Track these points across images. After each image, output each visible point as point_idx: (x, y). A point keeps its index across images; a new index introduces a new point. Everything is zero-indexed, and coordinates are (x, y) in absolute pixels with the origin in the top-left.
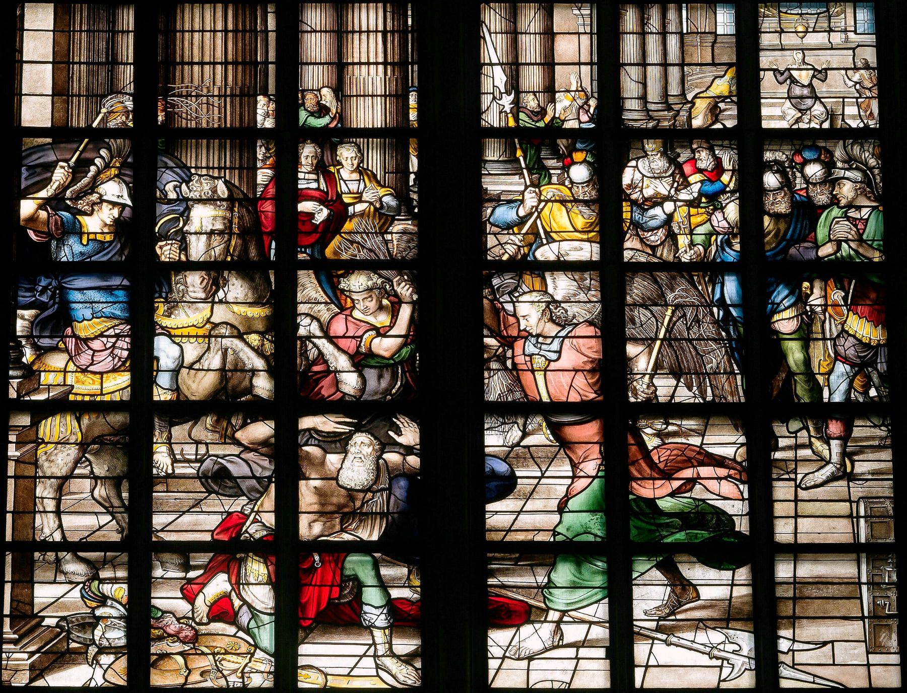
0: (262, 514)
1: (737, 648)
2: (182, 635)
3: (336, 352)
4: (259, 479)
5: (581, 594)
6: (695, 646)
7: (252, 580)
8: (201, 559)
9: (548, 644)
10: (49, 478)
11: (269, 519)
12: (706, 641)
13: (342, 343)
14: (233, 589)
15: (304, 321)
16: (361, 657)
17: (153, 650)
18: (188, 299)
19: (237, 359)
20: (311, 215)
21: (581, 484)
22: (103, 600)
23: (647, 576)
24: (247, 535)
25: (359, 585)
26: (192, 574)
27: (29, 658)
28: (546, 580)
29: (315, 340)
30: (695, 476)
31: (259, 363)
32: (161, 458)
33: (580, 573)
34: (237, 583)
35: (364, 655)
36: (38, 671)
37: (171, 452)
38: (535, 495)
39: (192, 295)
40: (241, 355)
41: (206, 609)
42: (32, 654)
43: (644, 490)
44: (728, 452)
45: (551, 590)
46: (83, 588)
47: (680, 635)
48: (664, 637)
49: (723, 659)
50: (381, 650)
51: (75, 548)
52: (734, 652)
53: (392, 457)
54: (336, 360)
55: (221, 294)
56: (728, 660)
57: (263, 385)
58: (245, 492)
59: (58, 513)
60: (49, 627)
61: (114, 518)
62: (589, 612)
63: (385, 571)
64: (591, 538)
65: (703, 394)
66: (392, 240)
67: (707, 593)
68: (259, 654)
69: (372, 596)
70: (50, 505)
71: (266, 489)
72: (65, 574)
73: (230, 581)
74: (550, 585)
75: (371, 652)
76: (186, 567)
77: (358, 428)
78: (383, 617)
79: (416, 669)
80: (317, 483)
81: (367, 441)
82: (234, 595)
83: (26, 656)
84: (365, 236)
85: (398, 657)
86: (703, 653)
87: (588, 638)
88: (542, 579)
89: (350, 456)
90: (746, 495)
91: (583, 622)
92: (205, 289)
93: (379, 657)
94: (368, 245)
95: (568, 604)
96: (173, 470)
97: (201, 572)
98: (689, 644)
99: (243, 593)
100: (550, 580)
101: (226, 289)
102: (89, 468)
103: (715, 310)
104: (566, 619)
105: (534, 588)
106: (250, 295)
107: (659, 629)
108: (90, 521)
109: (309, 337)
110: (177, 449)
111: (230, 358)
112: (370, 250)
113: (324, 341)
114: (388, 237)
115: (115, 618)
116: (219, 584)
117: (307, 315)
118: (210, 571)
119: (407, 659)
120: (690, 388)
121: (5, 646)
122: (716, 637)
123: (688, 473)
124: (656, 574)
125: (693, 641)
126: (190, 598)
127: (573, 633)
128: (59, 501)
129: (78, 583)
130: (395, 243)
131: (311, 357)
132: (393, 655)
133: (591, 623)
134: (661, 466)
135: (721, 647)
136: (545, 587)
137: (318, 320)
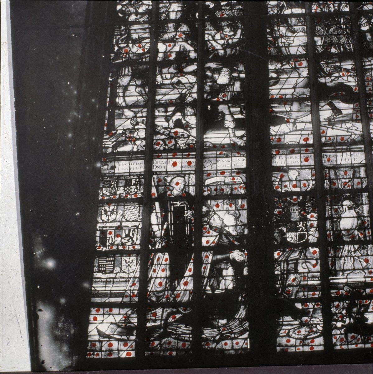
0: (192, 94)
1: (356, 128)
2: (165, 133)
3: (217, 44)
4: (191, 83)
5: (302, 113)
6: (342, 129)
7: (189, 114)
8: (171, 109)
9: (292, 130)
10: (122, 86)
11: (195, 96)
12: (346, 127)
13: (219, 42)
14: (182, 118)
15: (206, 36)
16: (225, 137)
17: (154, 138)
18: (169, 31)
19: (184, 48)
20: (209, 6)
21: (301, 79)
22: (137, 123)
23: (324, 108)
24: (187, 101)
25: (224, 115)
26: (168, 114)
27: (112, 143)
28: (289, 109)
29: (211, 41)
30: (339, 75)
31: (192, 49)
32: (159, 79)
33: (301, 106)
34: (184, 115)
35: (226, 137)
36: (115, 147)
37: (162, 77)
38: (286, 84)
39: (170, 30)
40: (186, 47)
41: (173, 124)
42: (113, 142)
43: (322, 80)
44: (350, 67)
45: (291, 113)
46: (131, 120)
47: (337, 126)
48: (331, 127)
49: (352, 132)
50: (232, 135)
51: (129, 107)
52: (356, 130)
53: (235, 75)
54: (217, 46)
55: (179, 29)
56: (353, 132)
57: (193, 55)
58: (187, 87)
59: (124, 97)
60: (119, 133)
61: (143, 97)
62: (305, 119)
63: (232, 110)
64: (305, 96)
65: (340, 50)
66: (234, 12)
67: (344, 112)
68: (191, 138)
69: (228, 118)
70: (121, 94)
71: (194, 86)
72: (126, 116)
73: (181, 115)
74: (291, 111)
75: (228, 136)
76: (166, 111)
77: (224, 66)
78: (232, 124)
79: (244, 141)
80: (210, 84)
81: (227, 70)
82: (183, 120)
83: (111, 143)
84: (226, 11)
85: (238, 137)
86: (345, 131)
87: (305, 127)
88: (288, 109)
89: (221, 75)
90: (356, 80)
91: (302, 122)
92: (174, 28)
93: (231, 137)
94: (227, 13)
95: (297, 117)
96: (162, 82)
97: (171, 113)
98: (340, 128)
99: (186, 119)
100: (291, 109)
101: (181, 28)
102: (135, 82)
103: (342, 26)
104: (296, 121)
105: (285, 112)
106: (189, 29)
107: (329, 124)
108: (135, 99)
109: (209, 40)
110: (164, 76)
111: (182, 48)
112: (228, 15)
113: (213, 41)
114: (233, 11)
115: (142, 129)
116: (178, 116)
117: (208, 34)
118: (174, 113)
119: (241, 137)
120: (336, 48)
121: (104, 141)
122: (349, 125)
123: (336, 75)
124: (327, 107)
125: (341, 127)
126: (167, 121)
127: (300, 126)
128: (124, 93)
129: (129, 119)
130: (235, 12)
131: (209, 46)
132: (236, 137)
133: (306, 122)
134: (327, 73)
135: (351, 128)
136: (289, 112)
137: (211, 35)
